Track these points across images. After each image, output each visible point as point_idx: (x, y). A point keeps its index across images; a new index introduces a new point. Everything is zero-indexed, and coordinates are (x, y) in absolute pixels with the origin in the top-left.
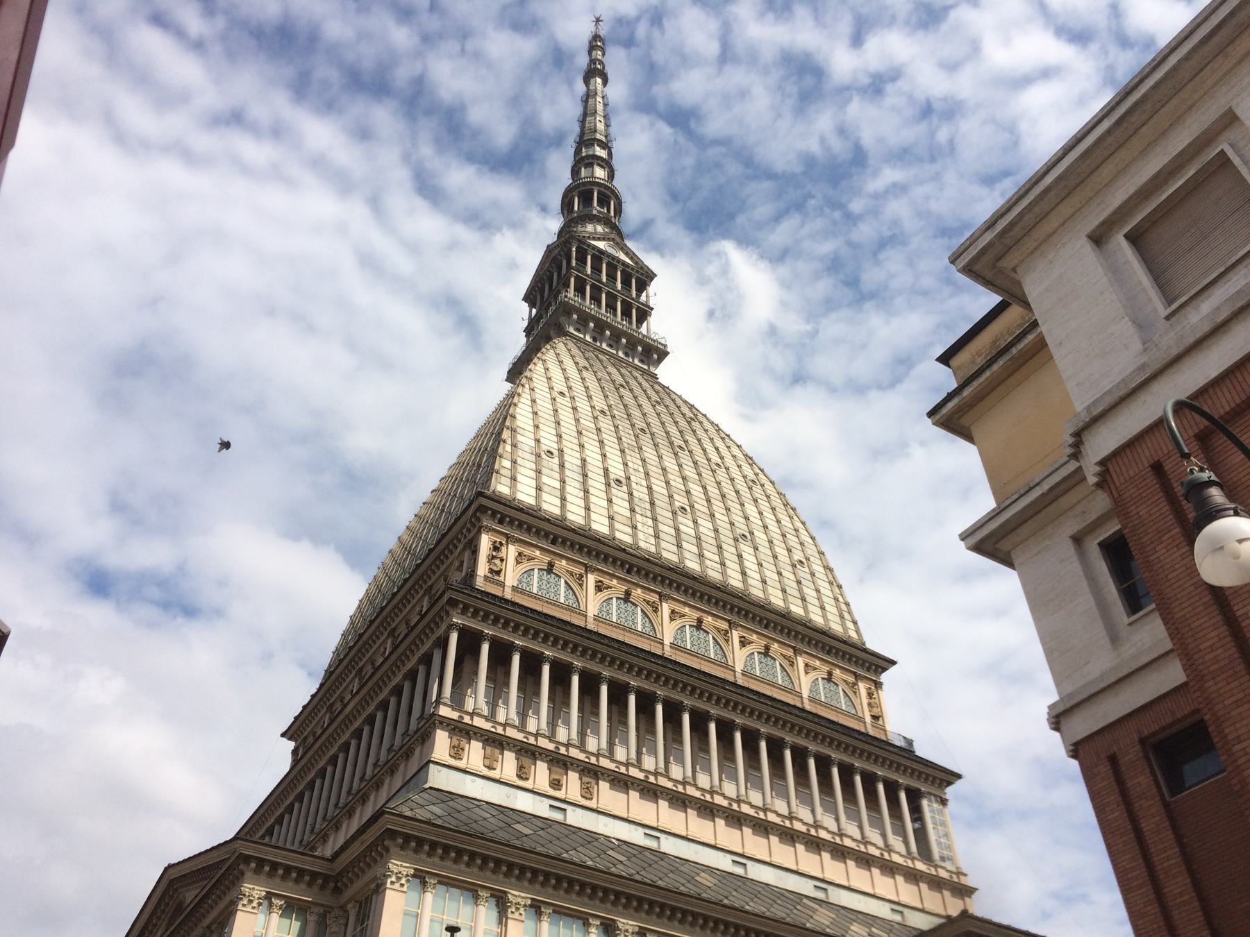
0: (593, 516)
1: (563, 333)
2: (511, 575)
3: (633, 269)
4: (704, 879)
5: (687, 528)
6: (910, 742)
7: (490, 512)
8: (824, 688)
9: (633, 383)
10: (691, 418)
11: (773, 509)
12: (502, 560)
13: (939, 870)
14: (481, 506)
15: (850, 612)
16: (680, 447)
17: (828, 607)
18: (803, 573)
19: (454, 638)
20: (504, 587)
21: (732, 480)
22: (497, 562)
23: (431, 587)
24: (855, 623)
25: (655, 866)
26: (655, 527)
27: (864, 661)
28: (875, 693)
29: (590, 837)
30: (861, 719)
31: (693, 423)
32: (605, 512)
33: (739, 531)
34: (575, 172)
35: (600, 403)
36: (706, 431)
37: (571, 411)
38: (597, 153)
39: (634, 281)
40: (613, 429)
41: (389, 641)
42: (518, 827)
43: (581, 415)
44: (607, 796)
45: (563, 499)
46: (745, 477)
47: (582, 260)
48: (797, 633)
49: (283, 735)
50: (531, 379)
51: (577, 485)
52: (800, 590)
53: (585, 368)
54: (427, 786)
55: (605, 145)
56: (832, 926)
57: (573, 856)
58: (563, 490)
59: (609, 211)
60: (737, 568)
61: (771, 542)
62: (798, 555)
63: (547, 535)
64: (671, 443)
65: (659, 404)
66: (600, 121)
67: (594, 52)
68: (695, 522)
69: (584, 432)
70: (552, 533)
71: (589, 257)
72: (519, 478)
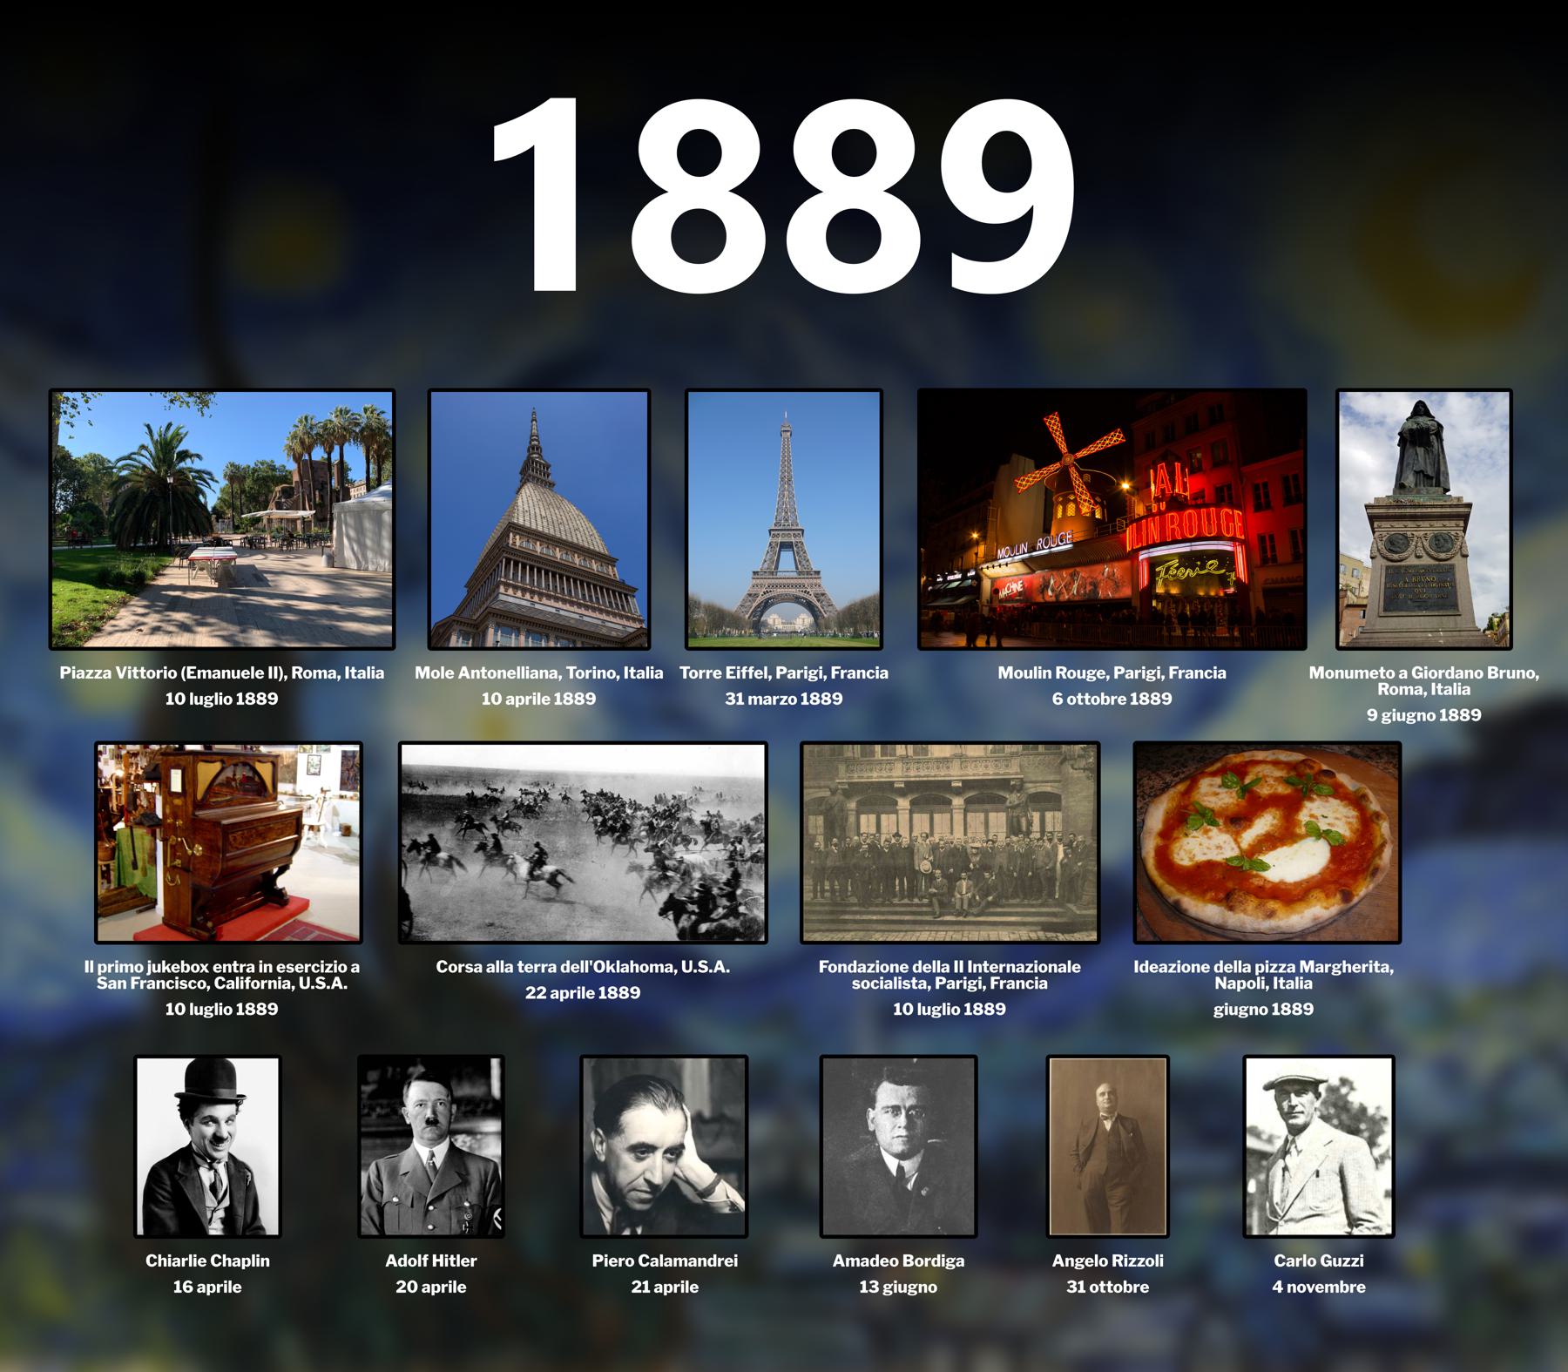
2: (518, 543)
4: (572, 621)
29: (542, 611)
44: (544, 600)
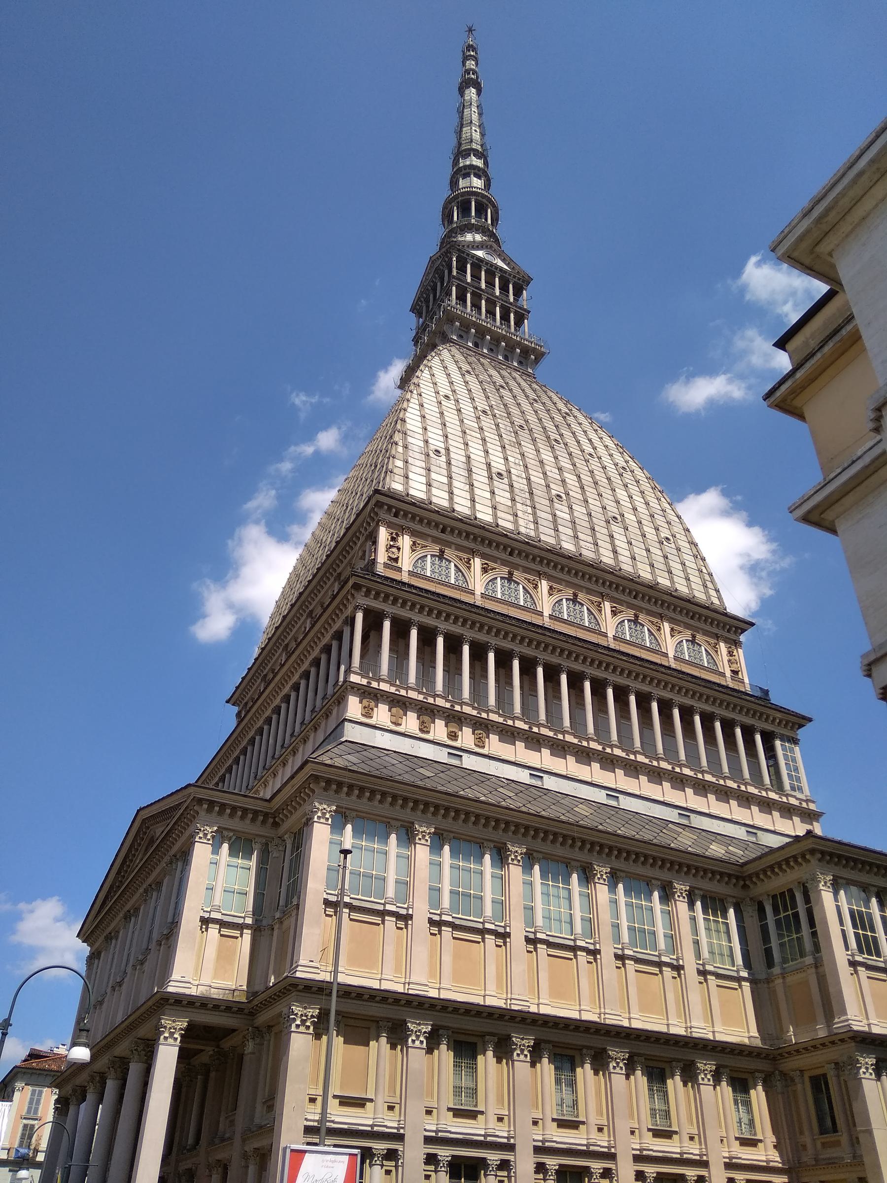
0: (478, 506)
1: (445, 339)
2: (407, 561)
3: (510, 275)
4: (582, 810)
5: (563, 514)
6: (766, 692)
7: (386, 507)
8: (688, 648)
9: (512, 383)
10: (566, 413)
11: (642, 492)
12: (399, 549)
13: (790, 798)
14: (378, 501)
15: (712, 581)
16: (556, 440)
17: (692, 578)
18: (670, 549)
19: (359, 617)
20: (401, 572)
21: (604, 468)
22: (394, 550)
23: (340, 574)
24: (717, 591)
25: (539, 799)
26: (534, 514)
27: (725, 624)
28: (735, 651)
29: (484, 777)
30: (723, 675)
31: (568, 418)
32: (489, 503)
33: (610, 514)
34: (454, 183)
35: (482, 404)
36: (580, 424)
37: (456, 412)
38: (474, 163)
39: (511, 286)
40: (494, 427)
41: (308, 621)
42: (421, 770)
43: (464, 416)
45: (451, 493)
46: (616, 465)
47: (462, 269)
48: (663, 602)
49: (227, 702)
50: (419, 386)
51: (463, 479)
52: (667, 564)
53: (468, 372)
54: (343, 739)
55: (478, 155)
56: (693, 846)
57: (470, 794)
58: (450, 484)
59: (486, 220)
60: (609, 547)
61: (639, 523)
62: (665, 533)
63: (437, 525)
64: (548, 437)
65: (537, 401)
66: (476, 131)
67: (468, 62)
68: (571, 508)
69: (467, 431)
70: (442, 524)
71: (469, 266)
72: (411, 475)
